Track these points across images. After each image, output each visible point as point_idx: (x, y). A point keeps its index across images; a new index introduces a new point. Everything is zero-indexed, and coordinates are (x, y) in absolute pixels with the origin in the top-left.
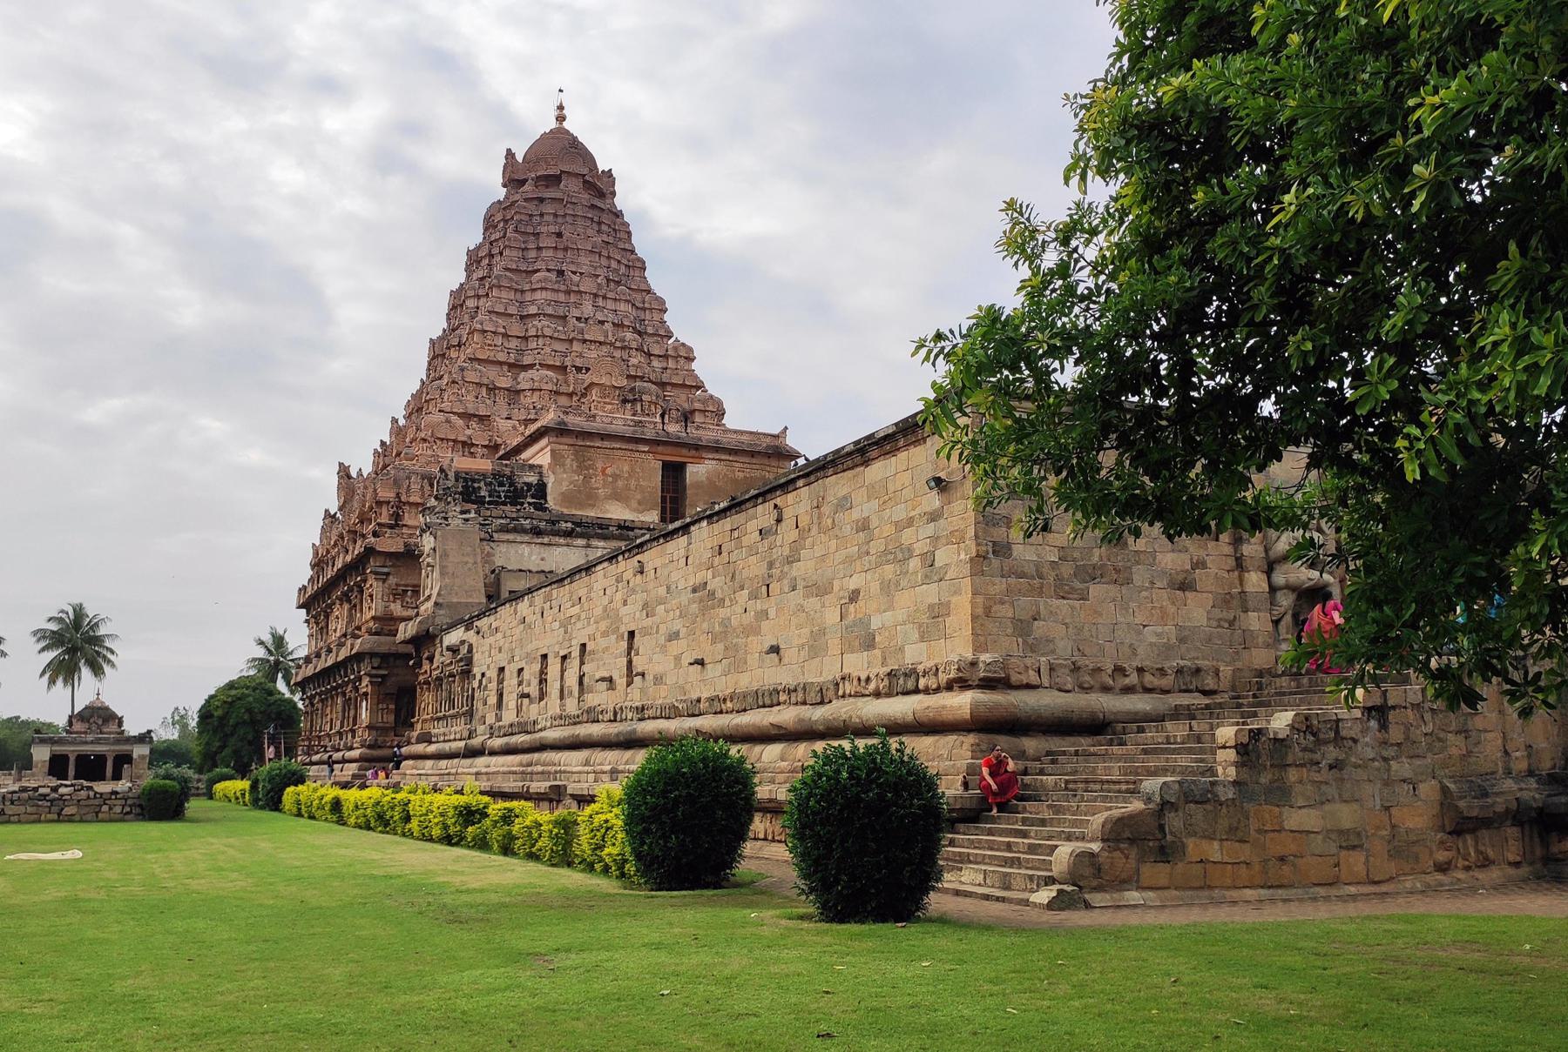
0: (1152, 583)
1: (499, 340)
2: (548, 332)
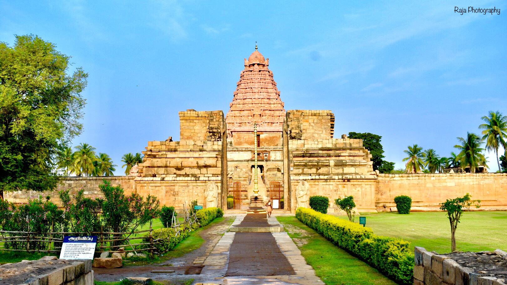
1: (238, 105)
2: (247, 103)
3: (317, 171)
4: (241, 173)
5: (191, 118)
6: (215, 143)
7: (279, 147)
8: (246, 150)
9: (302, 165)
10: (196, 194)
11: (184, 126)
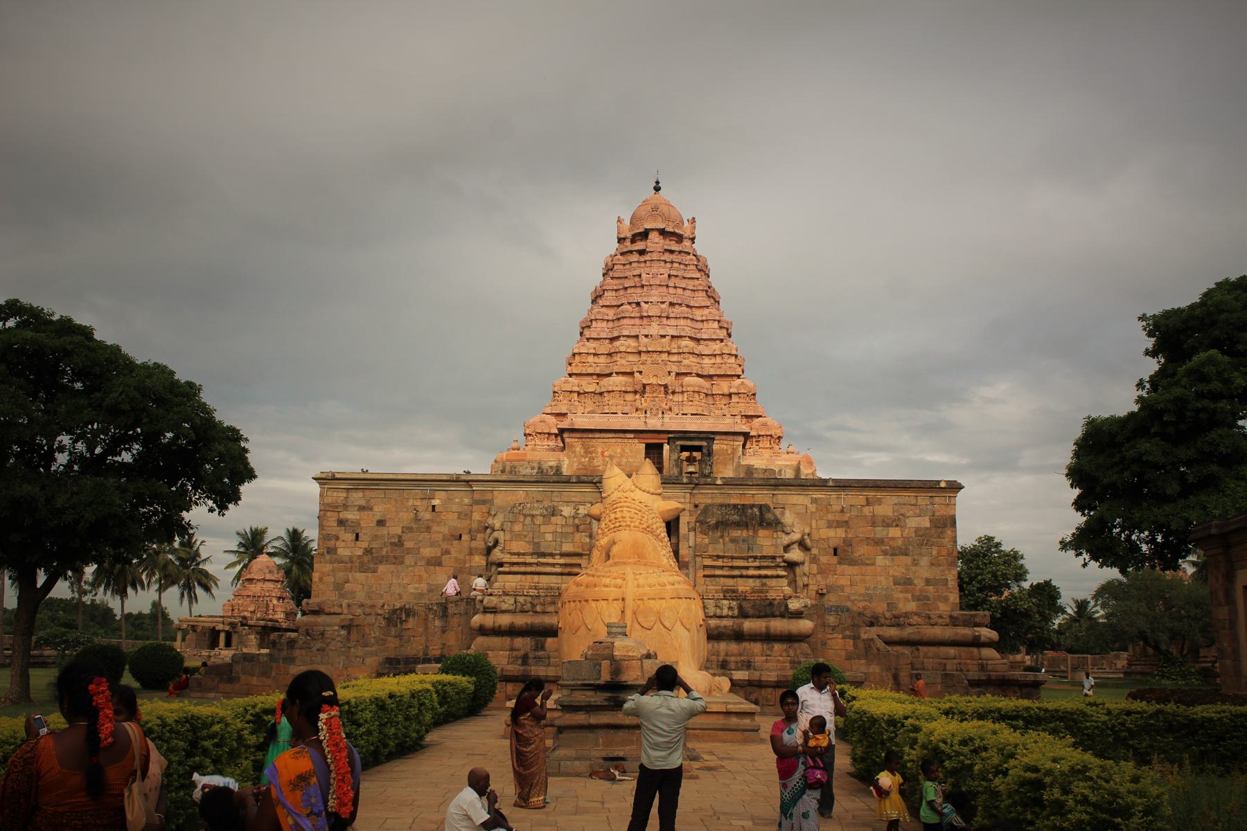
0: (416, 563)
1: (591, 359)
2: (622, 349)
4: (551, 528)
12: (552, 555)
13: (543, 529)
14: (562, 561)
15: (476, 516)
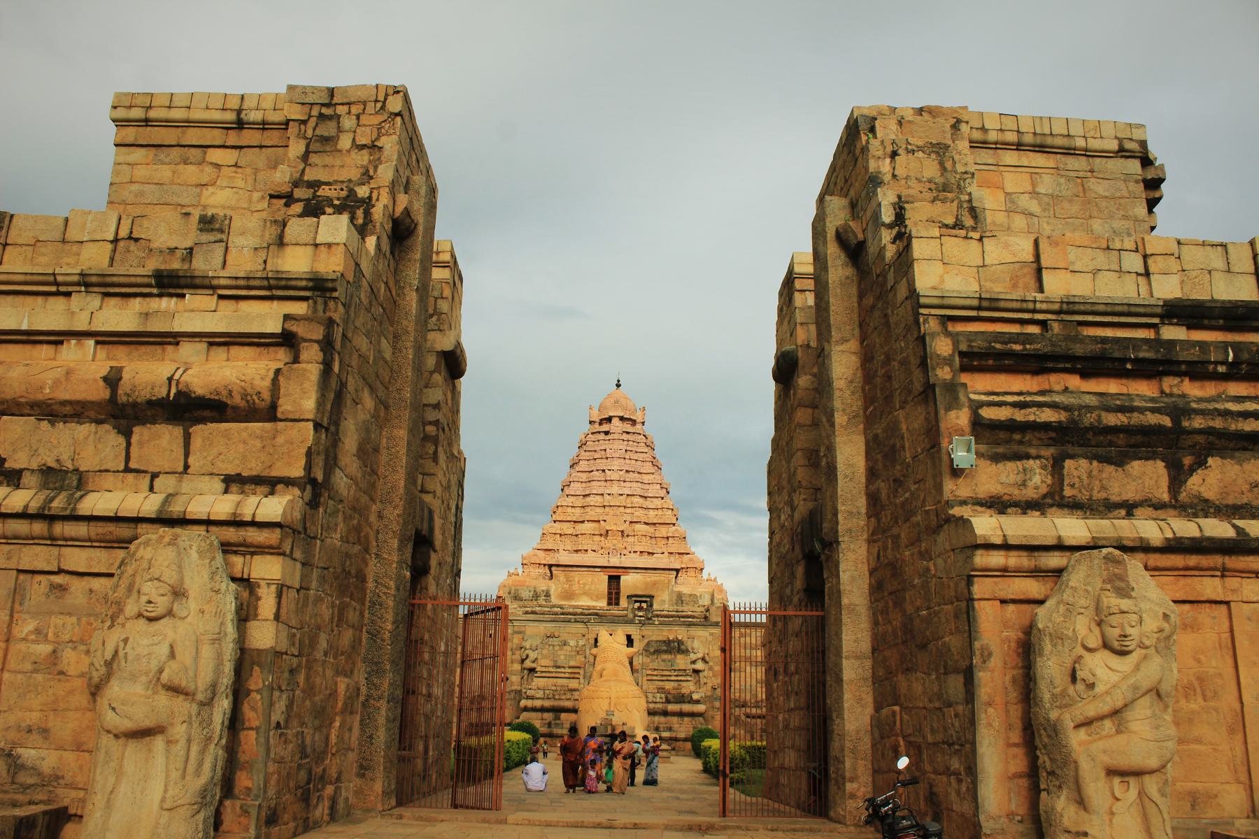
1: (569, 510)
2: (592, 504)
3: (1176, 483)
4: (563, 652)
5: (193, 136)
6: (298, 228)
7: (666, 607)
8: (586, 612)
9: (1046, 426)
10: (44, 649)
11: (134, 187)
12: (564, 667)
13: (559, 653)
14: (570, 670)
15: (516, 641)
